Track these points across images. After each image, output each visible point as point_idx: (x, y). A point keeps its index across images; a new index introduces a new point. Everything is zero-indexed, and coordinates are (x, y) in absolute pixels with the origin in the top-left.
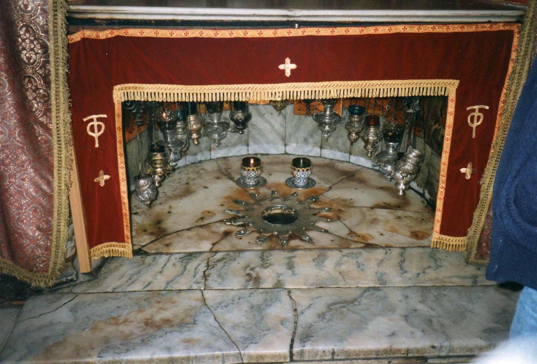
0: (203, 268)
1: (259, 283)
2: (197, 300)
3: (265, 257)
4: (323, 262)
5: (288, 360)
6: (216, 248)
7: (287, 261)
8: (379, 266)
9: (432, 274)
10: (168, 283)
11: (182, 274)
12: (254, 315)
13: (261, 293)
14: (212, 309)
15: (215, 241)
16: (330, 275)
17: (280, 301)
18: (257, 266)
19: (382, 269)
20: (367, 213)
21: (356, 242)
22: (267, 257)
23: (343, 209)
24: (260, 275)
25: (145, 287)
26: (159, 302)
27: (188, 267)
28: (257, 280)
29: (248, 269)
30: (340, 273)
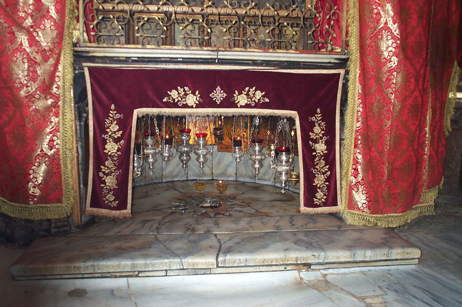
0: (156, 225)
5: (215, 266)
9: (311, 225)
17: (210, 238)
19: (278, 224)
27: (146, 225)
28: (194, 230)
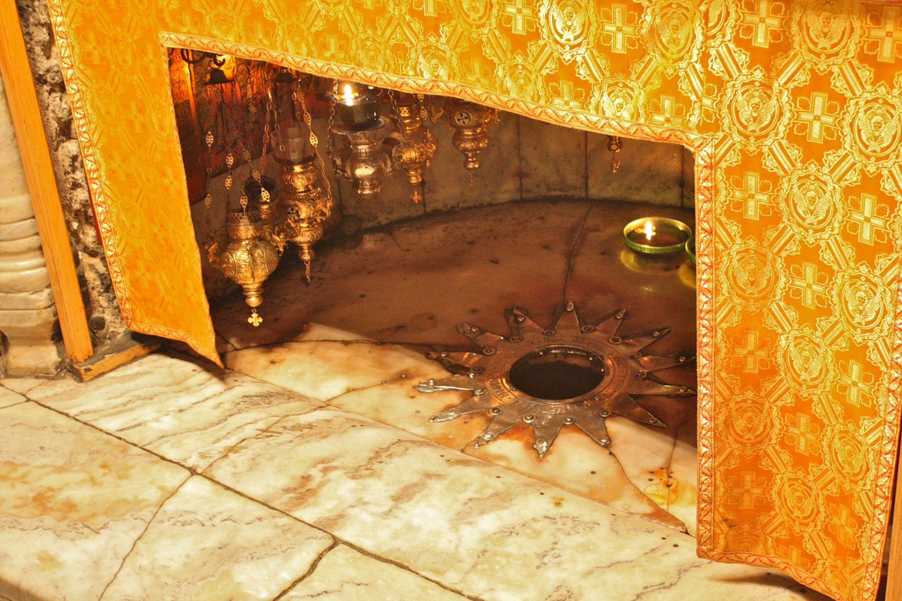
0: (250, 431)
1: (299, 505)
2: (162, 488)
3: (384, 455)
4: (482, 513)
6: (351, 401)
7: (416, 479)
8: (589, 573)
10: (163, 437)
11: (205, 429)
12: (205, 564)
13: (277, 526)
14: (159, 516)
15: (358, 382)
16: (457, 547)
18: (344, 468)
25: (122, 430)
26: (104, 466)
27: (231, 419)
29: (321, 466)
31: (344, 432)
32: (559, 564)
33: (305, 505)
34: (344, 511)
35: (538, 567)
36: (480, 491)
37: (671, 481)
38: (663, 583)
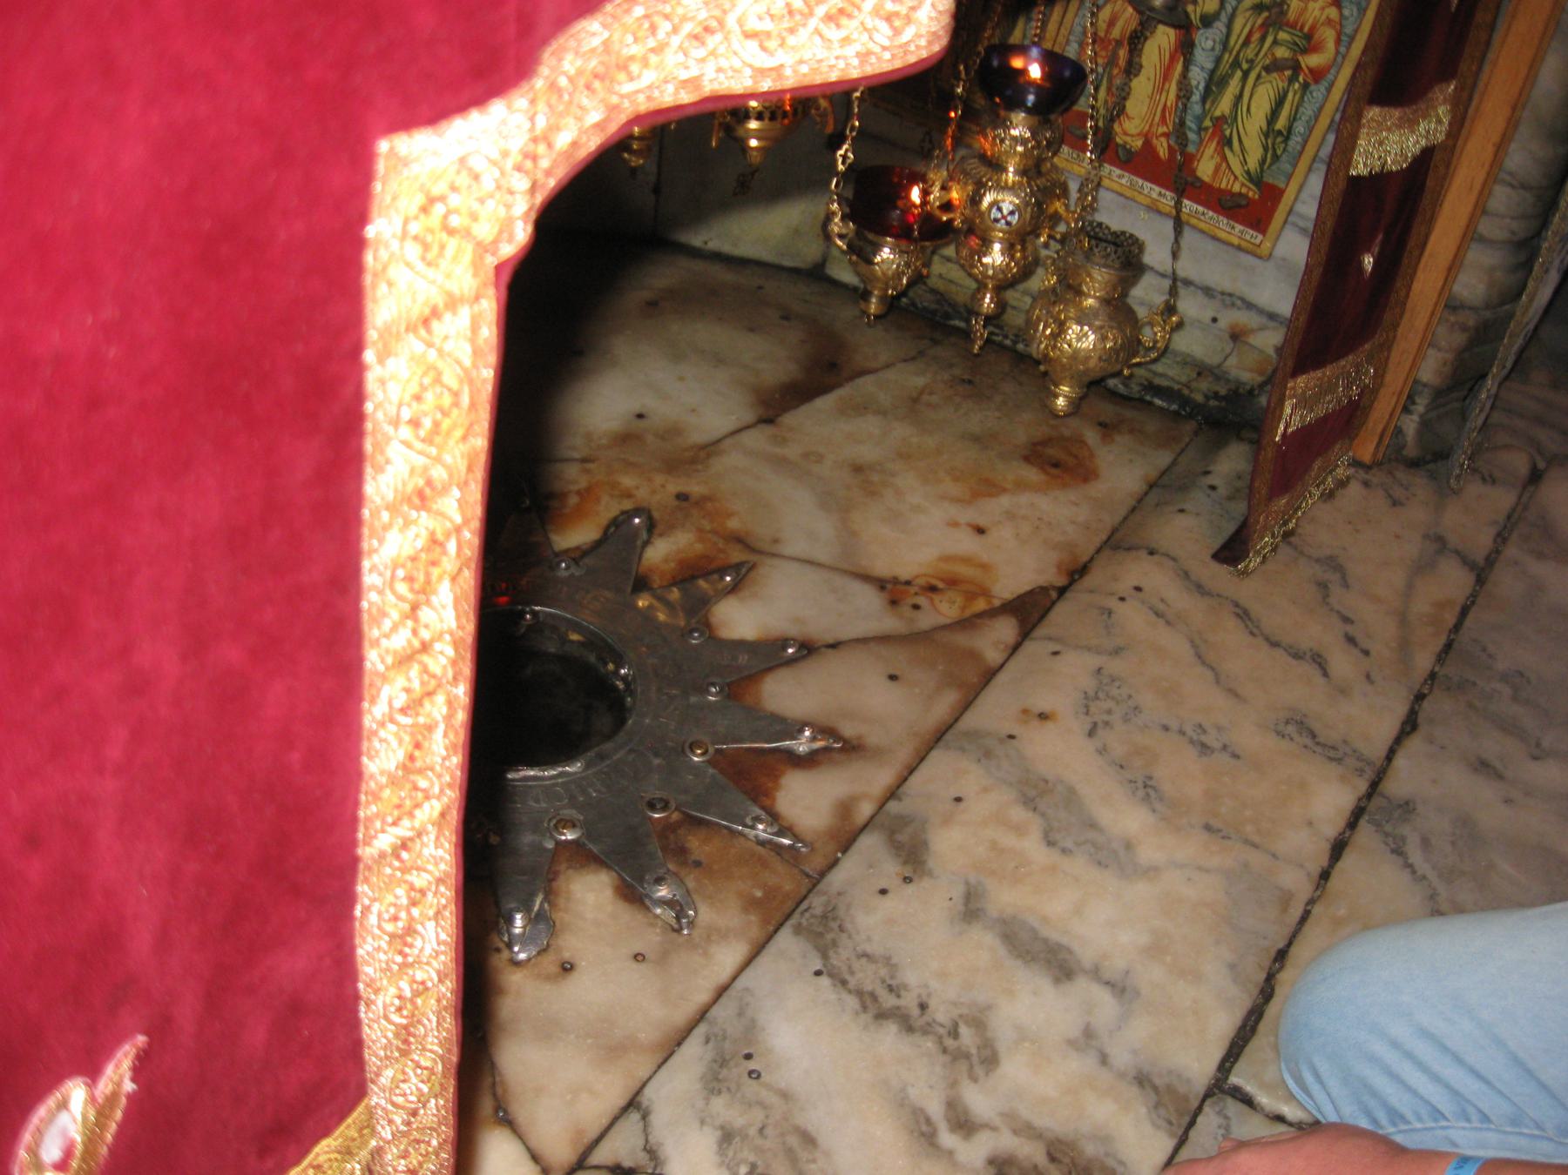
3: (889, 1001)
4: (1093, 825)
18: (954, 1084)
20: (792, 451)
21: (967, 623)
22: (891, 989)
23: (695, 488)
24: (1054, 1122)
29: (947, 1139)
30: (1208, 828)
31: (785, 1095)
32: (1219, 729)
33: (1111, 1162)
34: (1122, 1075)
35: (1236, 756)
36: (1019, 830)
37: (922, 581)
38: (1238, 615)
